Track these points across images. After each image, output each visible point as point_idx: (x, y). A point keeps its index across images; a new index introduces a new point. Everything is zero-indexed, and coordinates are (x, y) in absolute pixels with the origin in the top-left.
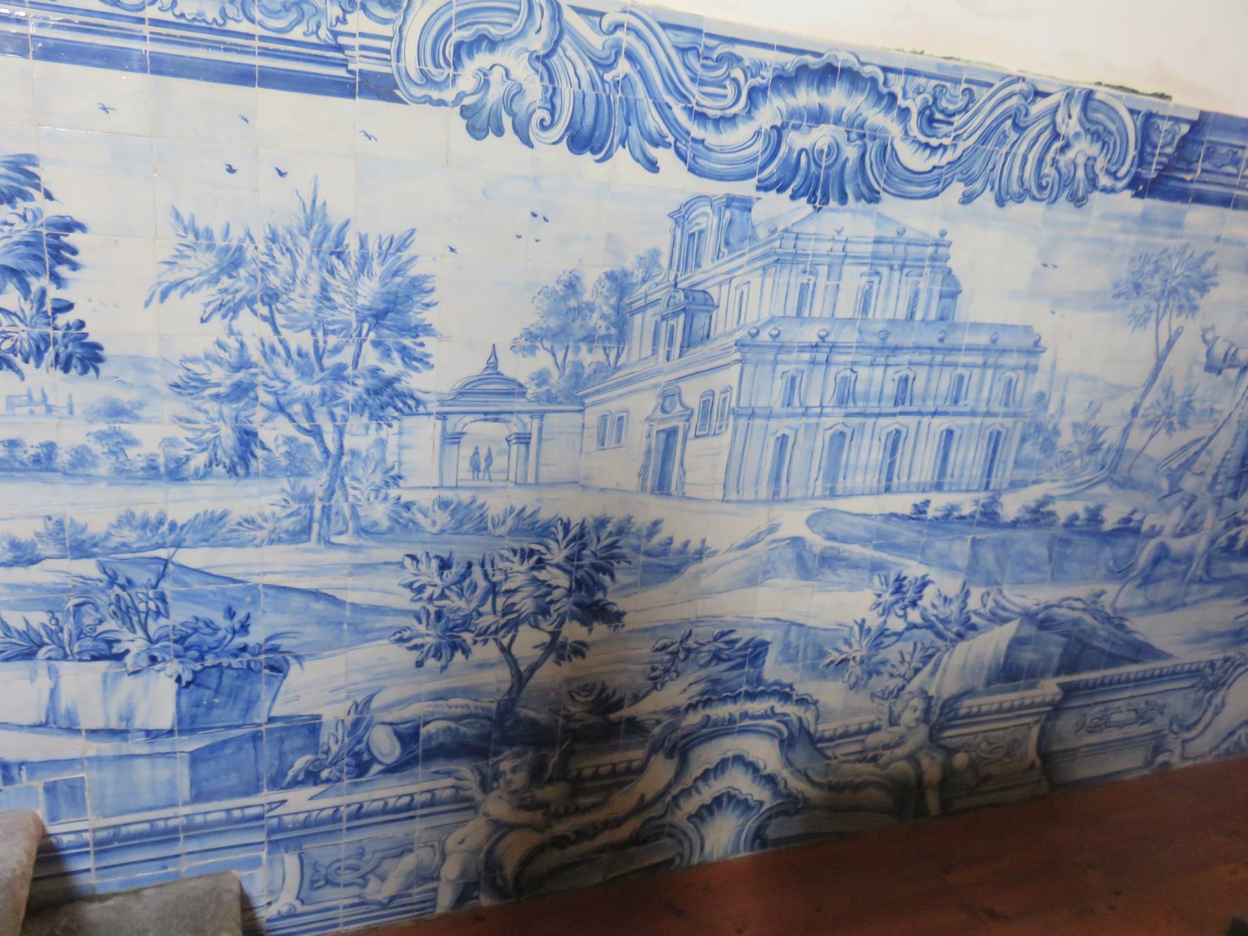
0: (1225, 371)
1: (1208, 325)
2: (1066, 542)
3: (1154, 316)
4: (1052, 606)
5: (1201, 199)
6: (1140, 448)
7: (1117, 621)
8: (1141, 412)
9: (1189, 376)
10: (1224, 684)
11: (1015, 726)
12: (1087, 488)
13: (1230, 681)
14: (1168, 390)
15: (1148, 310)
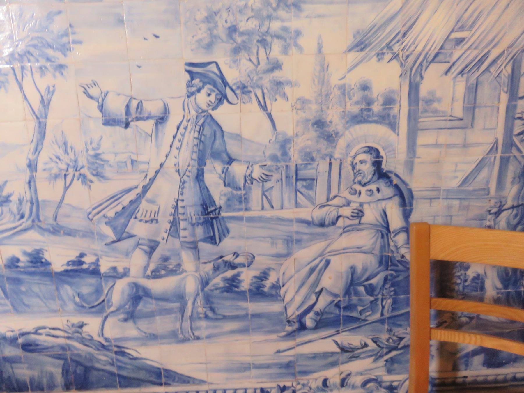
0: (132, 124)
1: (88, 80)
2: (17, 281)
3: (11, 78)
4: (28, 333)
7: (116, 349)
8: (40, 166)
12: (14, 234)
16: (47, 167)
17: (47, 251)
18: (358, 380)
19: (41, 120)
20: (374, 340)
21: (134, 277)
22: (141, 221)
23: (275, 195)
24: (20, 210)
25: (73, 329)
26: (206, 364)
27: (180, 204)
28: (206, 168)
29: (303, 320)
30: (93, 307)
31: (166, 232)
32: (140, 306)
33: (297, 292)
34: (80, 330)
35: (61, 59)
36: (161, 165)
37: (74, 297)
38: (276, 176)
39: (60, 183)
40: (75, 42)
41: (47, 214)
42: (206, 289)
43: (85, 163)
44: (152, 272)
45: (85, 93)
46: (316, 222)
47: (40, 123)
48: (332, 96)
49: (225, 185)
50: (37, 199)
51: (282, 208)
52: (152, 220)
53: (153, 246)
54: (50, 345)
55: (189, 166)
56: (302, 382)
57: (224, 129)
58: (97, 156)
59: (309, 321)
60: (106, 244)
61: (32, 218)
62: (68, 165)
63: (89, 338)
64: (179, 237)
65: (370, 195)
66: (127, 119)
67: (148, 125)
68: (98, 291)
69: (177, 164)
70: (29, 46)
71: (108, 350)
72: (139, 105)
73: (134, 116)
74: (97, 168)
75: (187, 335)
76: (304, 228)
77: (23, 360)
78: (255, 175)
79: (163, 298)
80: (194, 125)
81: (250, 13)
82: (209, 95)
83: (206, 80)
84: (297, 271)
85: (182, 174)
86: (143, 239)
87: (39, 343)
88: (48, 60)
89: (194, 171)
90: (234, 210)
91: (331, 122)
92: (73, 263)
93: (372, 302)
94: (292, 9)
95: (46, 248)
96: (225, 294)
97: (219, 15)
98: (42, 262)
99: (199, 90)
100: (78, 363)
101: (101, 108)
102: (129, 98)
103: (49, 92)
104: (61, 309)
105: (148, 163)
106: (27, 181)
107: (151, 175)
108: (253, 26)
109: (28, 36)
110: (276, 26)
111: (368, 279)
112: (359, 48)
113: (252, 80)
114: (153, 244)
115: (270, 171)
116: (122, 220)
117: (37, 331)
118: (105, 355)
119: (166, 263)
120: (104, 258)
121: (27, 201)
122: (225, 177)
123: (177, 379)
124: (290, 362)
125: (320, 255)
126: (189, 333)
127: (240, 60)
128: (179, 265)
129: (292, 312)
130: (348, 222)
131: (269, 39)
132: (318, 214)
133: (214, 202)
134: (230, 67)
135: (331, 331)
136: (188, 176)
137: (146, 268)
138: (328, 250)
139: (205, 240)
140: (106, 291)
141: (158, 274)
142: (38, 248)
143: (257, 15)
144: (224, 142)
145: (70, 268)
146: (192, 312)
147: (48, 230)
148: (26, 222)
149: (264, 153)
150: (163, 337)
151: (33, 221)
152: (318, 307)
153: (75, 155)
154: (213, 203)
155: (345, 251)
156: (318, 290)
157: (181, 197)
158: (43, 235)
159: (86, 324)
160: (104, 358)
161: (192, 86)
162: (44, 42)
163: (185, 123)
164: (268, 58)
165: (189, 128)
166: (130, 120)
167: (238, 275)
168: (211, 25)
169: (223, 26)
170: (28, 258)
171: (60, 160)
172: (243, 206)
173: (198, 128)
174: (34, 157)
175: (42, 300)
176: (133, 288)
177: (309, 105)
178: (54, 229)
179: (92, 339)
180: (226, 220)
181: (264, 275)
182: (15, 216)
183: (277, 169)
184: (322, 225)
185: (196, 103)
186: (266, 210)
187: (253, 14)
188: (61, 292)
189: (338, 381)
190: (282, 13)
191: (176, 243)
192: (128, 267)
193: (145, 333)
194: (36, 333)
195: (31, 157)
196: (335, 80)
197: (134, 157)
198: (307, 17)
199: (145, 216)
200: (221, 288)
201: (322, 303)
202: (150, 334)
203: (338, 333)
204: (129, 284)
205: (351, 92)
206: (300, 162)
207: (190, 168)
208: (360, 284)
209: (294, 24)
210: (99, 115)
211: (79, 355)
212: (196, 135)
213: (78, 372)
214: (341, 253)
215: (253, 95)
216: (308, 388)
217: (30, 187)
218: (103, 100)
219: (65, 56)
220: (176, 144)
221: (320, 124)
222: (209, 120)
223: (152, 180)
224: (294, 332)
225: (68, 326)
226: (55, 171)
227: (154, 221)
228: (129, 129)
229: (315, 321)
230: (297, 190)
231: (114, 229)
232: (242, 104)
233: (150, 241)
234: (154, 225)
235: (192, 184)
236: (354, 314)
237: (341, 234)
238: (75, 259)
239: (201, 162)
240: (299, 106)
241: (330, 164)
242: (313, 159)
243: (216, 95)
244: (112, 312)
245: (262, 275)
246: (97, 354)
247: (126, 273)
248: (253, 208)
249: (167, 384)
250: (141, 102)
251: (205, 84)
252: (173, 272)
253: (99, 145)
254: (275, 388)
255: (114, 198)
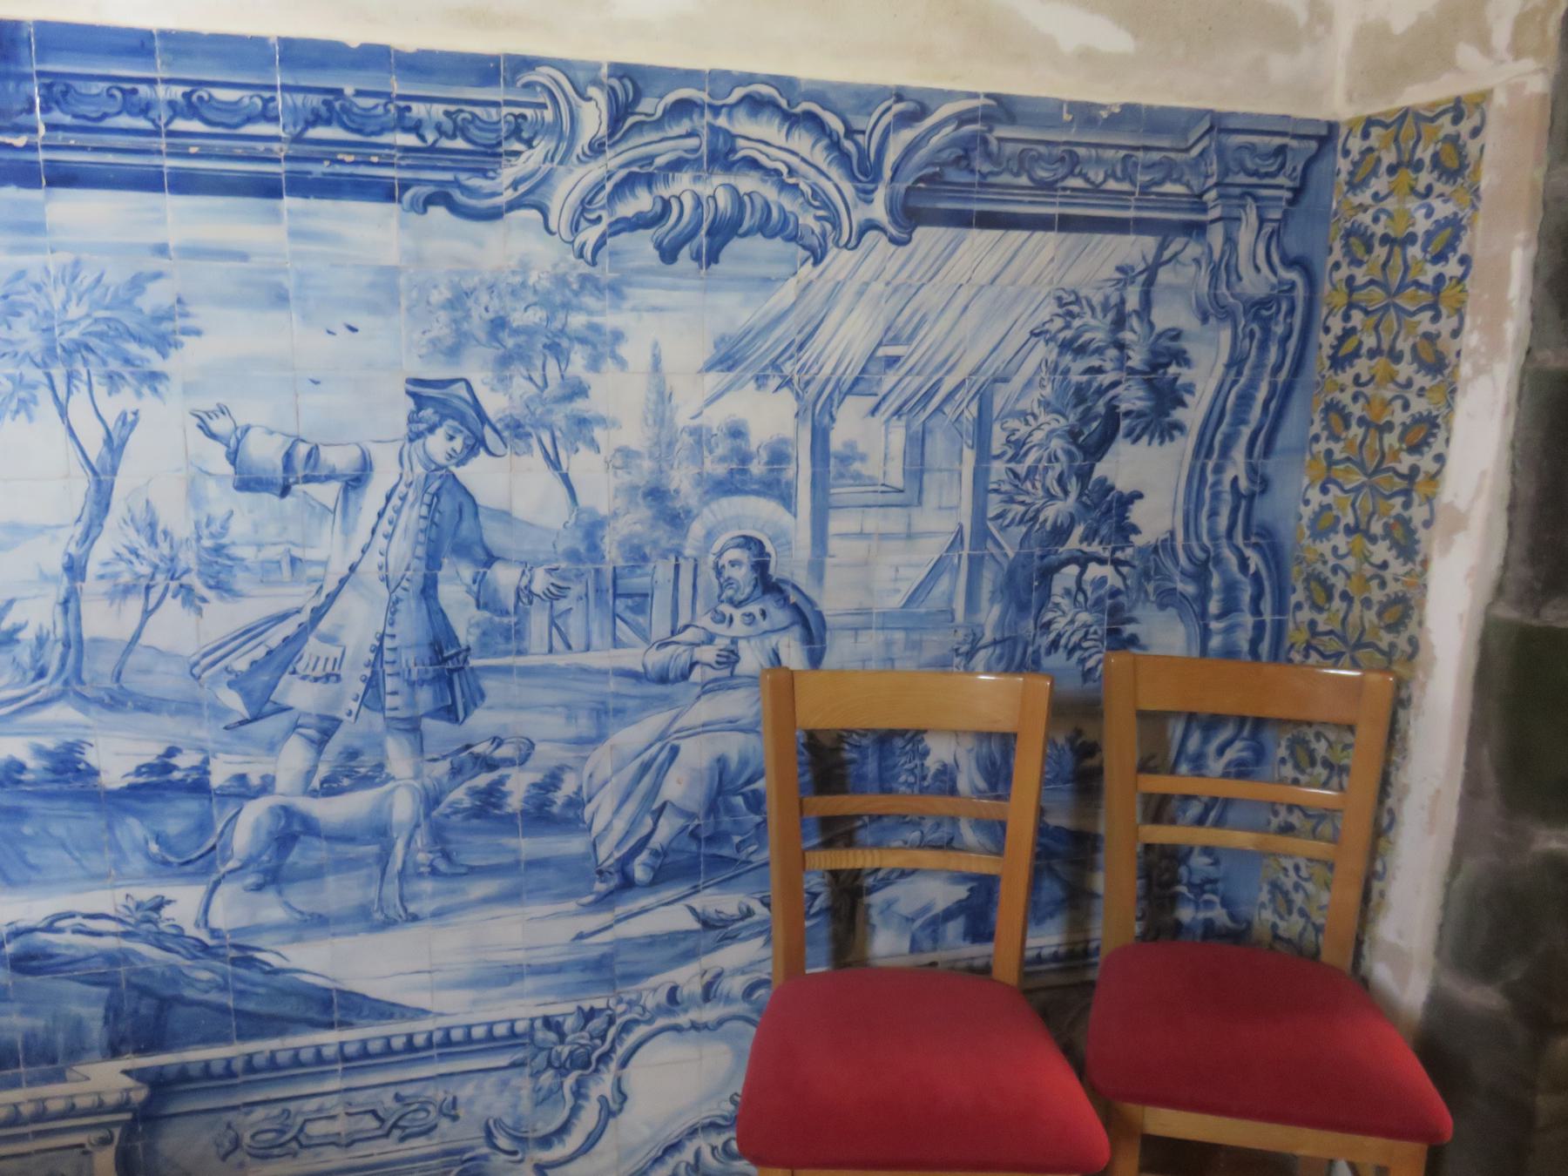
0: (295, 488)
1: (209, 404)
3: (44, 394)
4: (31, 930)
5: (64, 178)
6: (128, 636)
7: (233, 953)
8: (93, 568)
9: (195, 498)
10: (605, 1058)
11: (38, 1152)
12: (19, 711)
13: (621, 1051)
14: (151, 529)
15: (19, 382)
16: (109, 569)
17: (91, 745)
18: (736, 985)
19: (102, 478)
20: (766, 900)
21: (282, 794)
22: (304, 678)
23: (575, 625)
24: (37, 661)
25: (139, 915)
26: (429, 972)
27: (388, 643)
28: (441, 574)
29: (628, 868)
30: (188, 863)
31: (356, 700)
32: (294, 856)
33: (616, 812)
34: (155, 916)
35: (156, 363)
36: (352, 568)
37: (147, 843)
38: (576, 589)
39: (135, 606)
40: (186, 332)
41: (99, 668)
42: (434, 814)
43: (194, 565)
44: (322, 783)
45: (200, 427)
46: (653, 675)
47: (99, 483)
48: (678, 446)
49: (478, 606)
50: (80, 636)
51: (588, 649)
52: (327, 677)
53: (327, 728)
54: (81, 954)
55: (408, 569)
56: (626, 997)
57: (479, 501)
58: (218, 550)
59: (640, 872)
60: (226, 728)
61: (63, 677)
62: (156, 567)
63: (174, 931)
64: (383, 709)
65: (750, 624)
66: (286, 479)
67: (328, 493)
68: (203, 826)
69: (383, 567)
70: (90, 334)
71: (216, 956)
72: (313, 454)
73: (301, 473)
74: (219, 572)
75: (391, 913)
76: (627, 687)
77: (11, 995)
78: (538, 587)
79: (344, 836)
80: (420, 493)
81: (532, 298)
82: (451, 438)
83: (446, 410)
84: (617, 771)
85: (393, 586)
86: (309, 714)
87: (57, 951)
88: (127, 361)
89: (419, 579)
90: (496, 654)
91: (677, 491)
92: (150, 768)
93: (758, 825)
94: (607, 293)
95: (92, 741)
96: (475, 822)
97: (473, 298)
98: (78, 770)
99: (432, 429)
100: (144, 991)
101: (233, 457)
102: (291, 440)
103: (124, 423)
104: (113, 872)
105: (324, 564)
106: (61, 599)
107: (330, 587)
108: (537, 320)
109: (88, 315)
110: (577, 321)
111: (750, 781)
112: (725, 366)
113: (533, 414)
114: (326, 724)
115: (564, 579)
116: (265, 678)
117: (52, 923)
118: (206, 969)
119: (353, 764)
120: (221, 756)
121: (56, 641)
122: (479, 592)
123: (365, 1012)
124: (604, 956)
125: (660, 739)
126: (395, 910)
127: (511, 378)
128: (380, 766)
129: (607, 852)
130: (711, 674)
131: (565, 343)
132: (656, 659)
133: (456, 638)
134: (493, 390)
135: (684, 889)
136: (405, 589)
137: (311, 773)
138: (677, 726)
139: (434, 714)
140: (219, 827)
141: (335, 785)
142: (70, 739)
143: (544, 301)
144: (479, 526)
145: (141, 780)
146: (404, 862)
147: (100, 702)
148: (48, 686)
149: (554, 545)
150: (340, 920)
151: (66, 683)
152: (659, 839)
153: (172, 547)
154: (453, 639)
155: (706, 727)
156: (656, 806)
157: (389, 630)
158: (85, 711)
159: (169, 902)
160: (205, 975)
161: (419, 421)
162: (121, 328)
163: (402, 488)
164: (562, 377)
165: (411, 498)
166: (291, 480)
167: (501, 781)
168: (459, 314)
169: (481, 317)
170: (45, 763)
171: (138, 556)
172: (513, 645)
173: (427, 499)
174: (82, 551)
175: (70, 854)
176: (279, 817)
177: (638, 462)
178: (112, 698)
179: (180, 934)
180: (478, 673)
181: (553, 780)
182: (25, 673)
183: (579, 575)
184: (663, 679)
185: (425, 452)
186: (558, 653)
187: (535, 299)
188: (118, 833)
189: (696, 988)
190: (589, 301)
191: (377, 720)
192: (271, 773)
193: (301, 913)
194: (50, 928)
195: (73, 549)
196: (683, 418)
197: (297, 552)
198: (634, 309)
199: (314, 669)
200: (466, 810)
201: (666, 830)
202: (312, 915)
203: (696, 890)
204: (271, 810)
205: (713, 440)
206: (621, 563)
207: (409, 574)
208: (735, 793)
209: (610, 320)
210: (228, 469)
211: (147, 973)
212: (424, 511)
213: (143, 1011)
214: (698, 733)
215: (534, 442)
216: (638, 1009)
217: (66, 611)
218: (239, 441)
219: (164, 356)
220: (385, 526)
221: (656, 494)
222: (450, 483)
223: (332, 597)
224: (611, 893)
225: (126, 907)
226: (126, 578)
227: (333, 678)
228: (289, 499)
229: (653, 868)
230: (615, 615)
231: (246, 695)
232: (514, 456)
233: (322, 718)
234: (332, 687)
235: (413, 604)
236: (726, 852)
237: (699, 697)
238: (156, 762)
239: (433, 561)
240: (618, 463)
241: (677, 567)
242: (645, 558)
243: (465, 439)
244: (231, 872)
245: (548, 780)
246: (189, 967)
247: (266, 787)
248: (532, 651)
249: (345, 1024)
250: (317, 447)
251: (443, 418)
252: (366, 781)
253: (225, 528)
254: (571, 1014)
255: (251, 633)
